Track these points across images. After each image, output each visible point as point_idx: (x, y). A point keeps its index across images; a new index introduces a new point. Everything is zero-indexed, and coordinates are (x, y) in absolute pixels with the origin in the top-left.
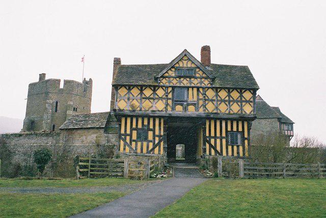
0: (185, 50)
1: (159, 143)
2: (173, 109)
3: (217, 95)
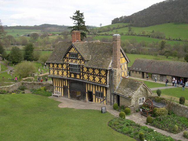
2: (70, 76)
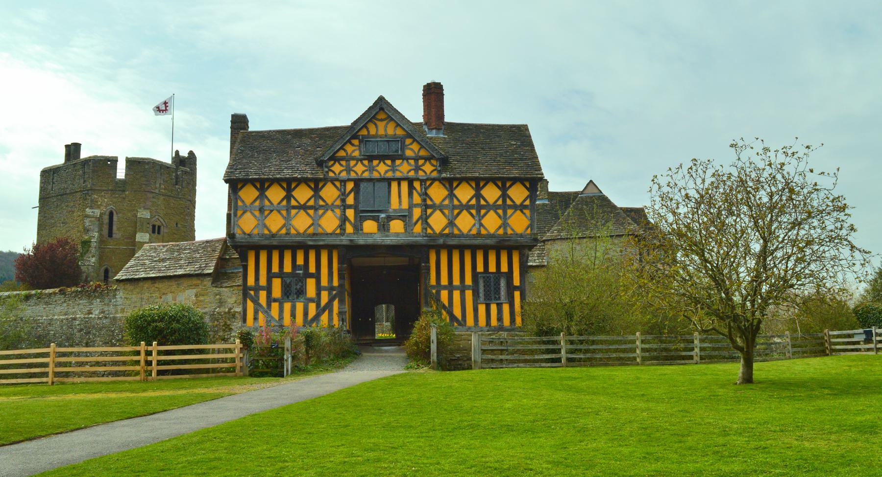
0: (381, 99)
1: (329, 305)
2: (358, 228)
3: (451, 196)
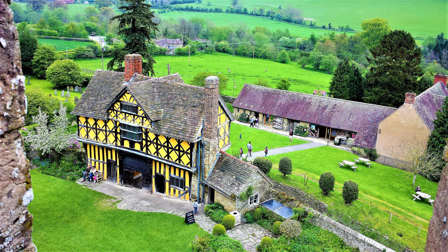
2: (122, 143)
